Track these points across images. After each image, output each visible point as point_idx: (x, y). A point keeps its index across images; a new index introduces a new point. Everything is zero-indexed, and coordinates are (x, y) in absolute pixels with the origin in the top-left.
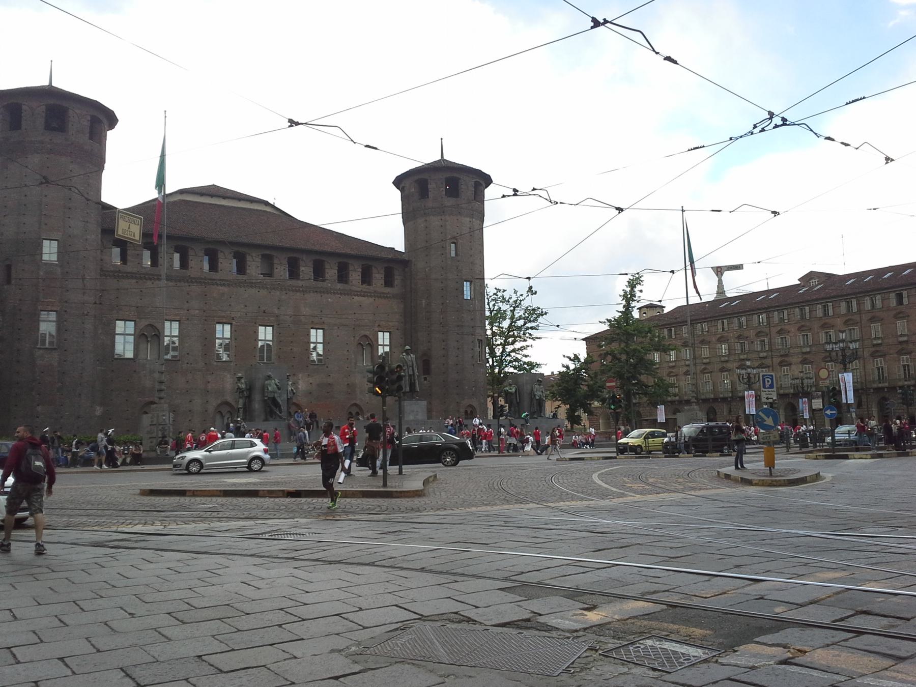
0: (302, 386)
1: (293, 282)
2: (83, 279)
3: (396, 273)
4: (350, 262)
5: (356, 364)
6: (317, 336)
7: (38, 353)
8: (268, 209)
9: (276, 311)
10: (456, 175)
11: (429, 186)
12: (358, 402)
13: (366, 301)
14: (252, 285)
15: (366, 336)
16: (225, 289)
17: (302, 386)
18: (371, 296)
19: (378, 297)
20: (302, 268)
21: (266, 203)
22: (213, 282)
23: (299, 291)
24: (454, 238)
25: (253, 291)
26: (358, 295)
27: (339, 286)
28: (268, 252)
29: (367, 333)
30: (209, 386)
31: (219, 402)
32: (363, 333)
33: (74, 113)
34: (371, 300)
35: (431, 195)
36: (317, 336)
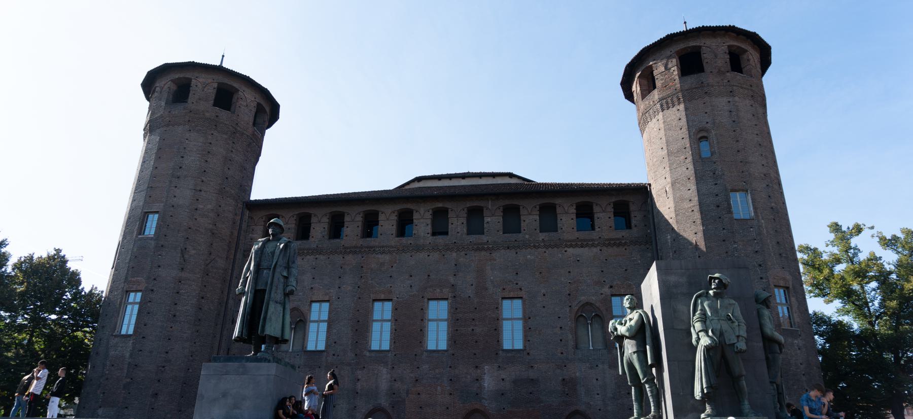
0: (489, 382)
1: (473, 238)
2: (184, 251)
3: (632, 207)
4: (558, 201)
5: (576, 347)
6: (512, 309)
7: (113, 341)
8: (514, 181)
9: (452, 280)
10: (692, 43)
11: (655, 73)
12: (582, 408)
13: (586, 253)
14: (419, 248)
15: (587, 304)
16: (387, 257)
17: (489, 382)
18: (593, 245)
19: (604, 245)
20: (487, 219)
21: (511, 175)
22: (371, 249)
23: (483, 249)
24: (701, 130)
25: (422, 255)
26: (571, 246)
27: (542, 236)
28: (440, 205)
29: (593, 299)
30: (359, 386)
31: (371, 407)
32: (583, 299)
33: (248, 98)
34: (595, 250)
35: (658, 83)
36: (512, 309)
